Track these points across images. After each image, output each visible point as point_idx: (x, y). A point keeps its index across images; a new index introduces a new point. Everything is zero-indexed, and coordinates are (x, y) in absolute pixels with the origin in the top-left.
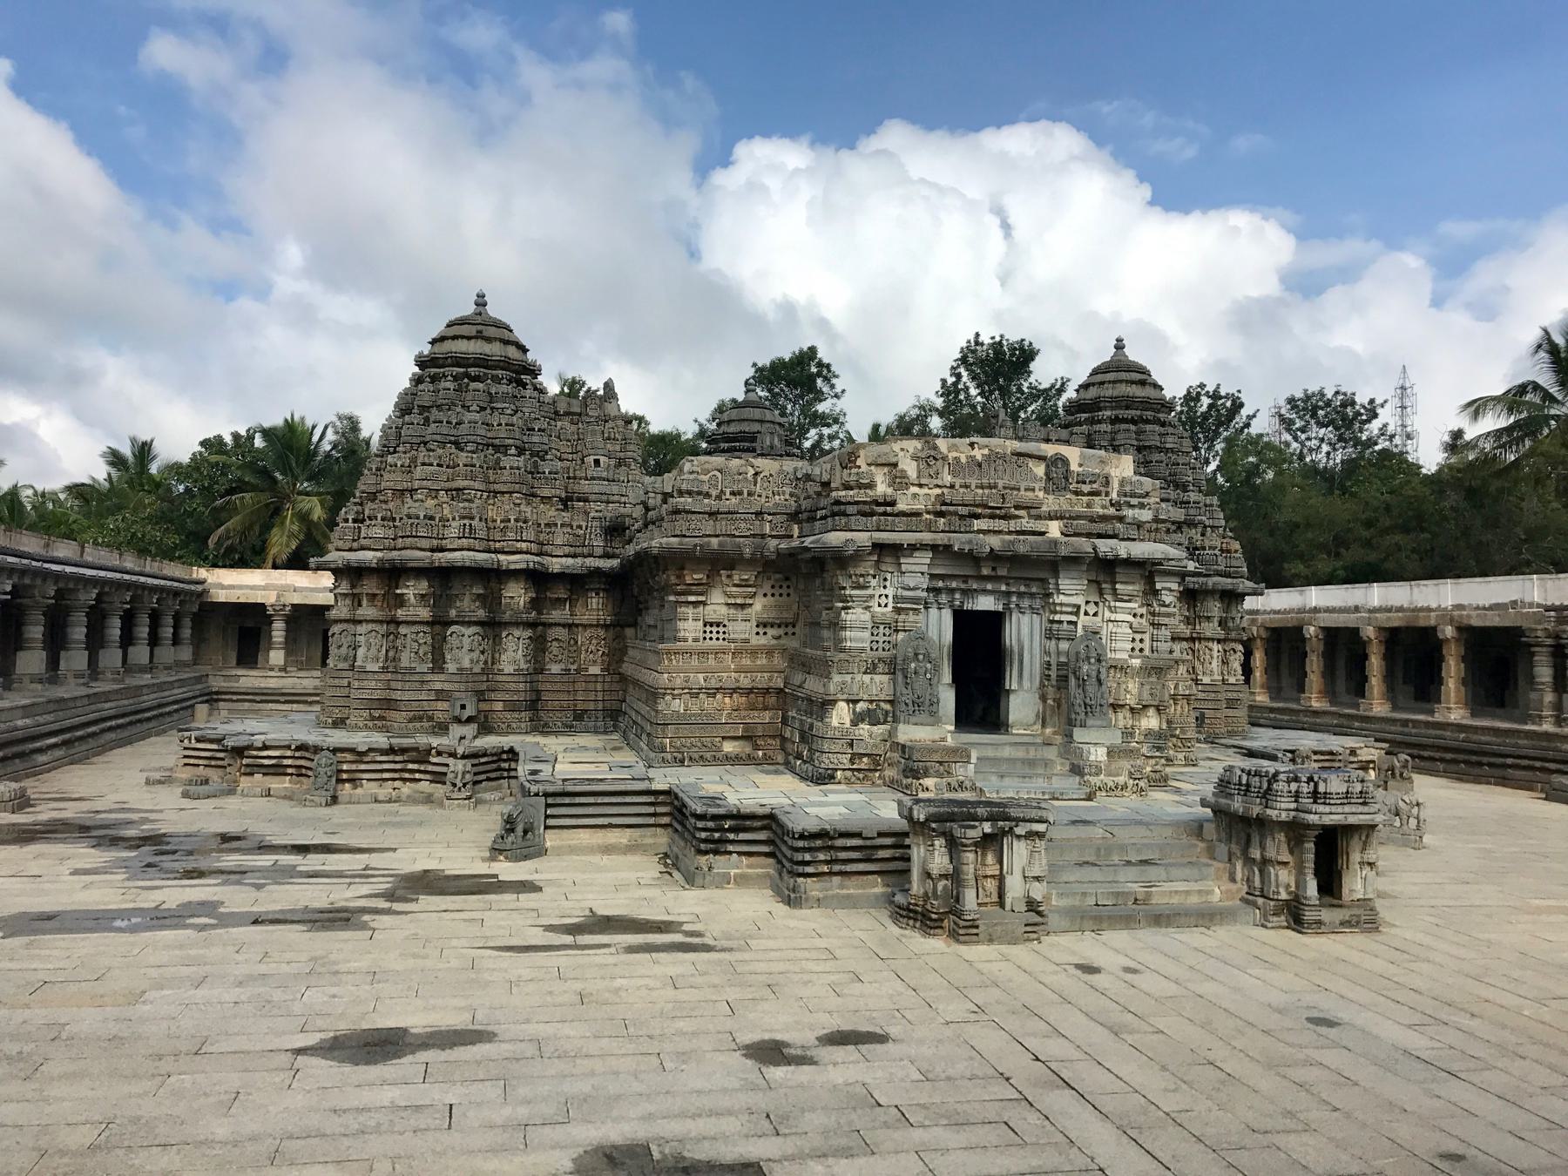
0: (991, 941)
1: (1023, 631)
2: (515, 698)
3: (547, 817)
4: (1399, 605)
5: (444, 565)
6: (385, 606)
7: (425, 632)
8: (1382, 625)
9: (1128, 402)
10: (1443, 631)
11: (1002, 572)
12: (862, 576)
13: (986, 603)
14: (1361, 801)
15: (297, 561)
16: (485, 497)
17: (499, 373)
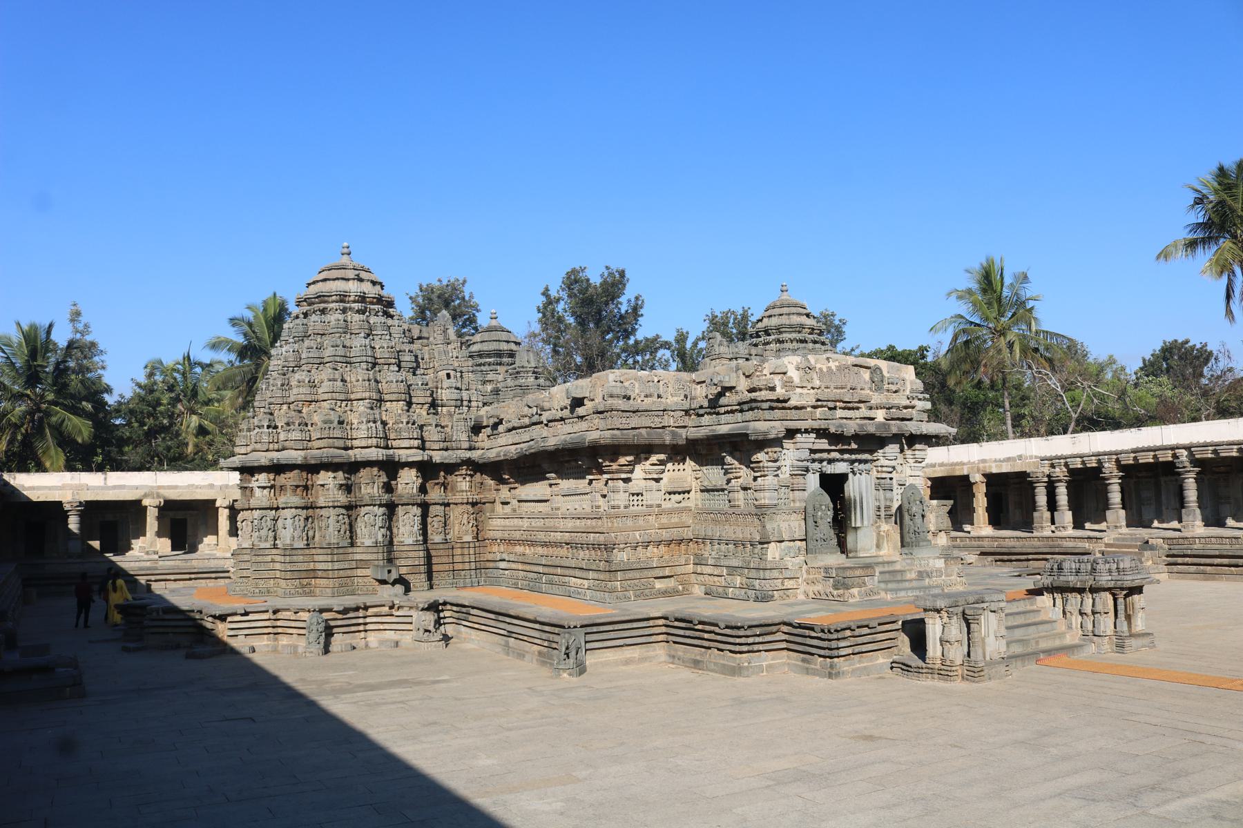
0: (990, 679)
1: (859, 486)
2: (417, 563)
3: (586, 642)
4: (941, 462)
5: (359, 460)
6: (305, 494)
7: (344, 515)
8: (930, 476)
9: (802, 326)
10: (974, 477)
11: (854, 446)
12: (775, 452)
13: (841, 468)
14: (1137, 571)
15: (212, 465)
16: (378, 405)
17: (376, 307)
